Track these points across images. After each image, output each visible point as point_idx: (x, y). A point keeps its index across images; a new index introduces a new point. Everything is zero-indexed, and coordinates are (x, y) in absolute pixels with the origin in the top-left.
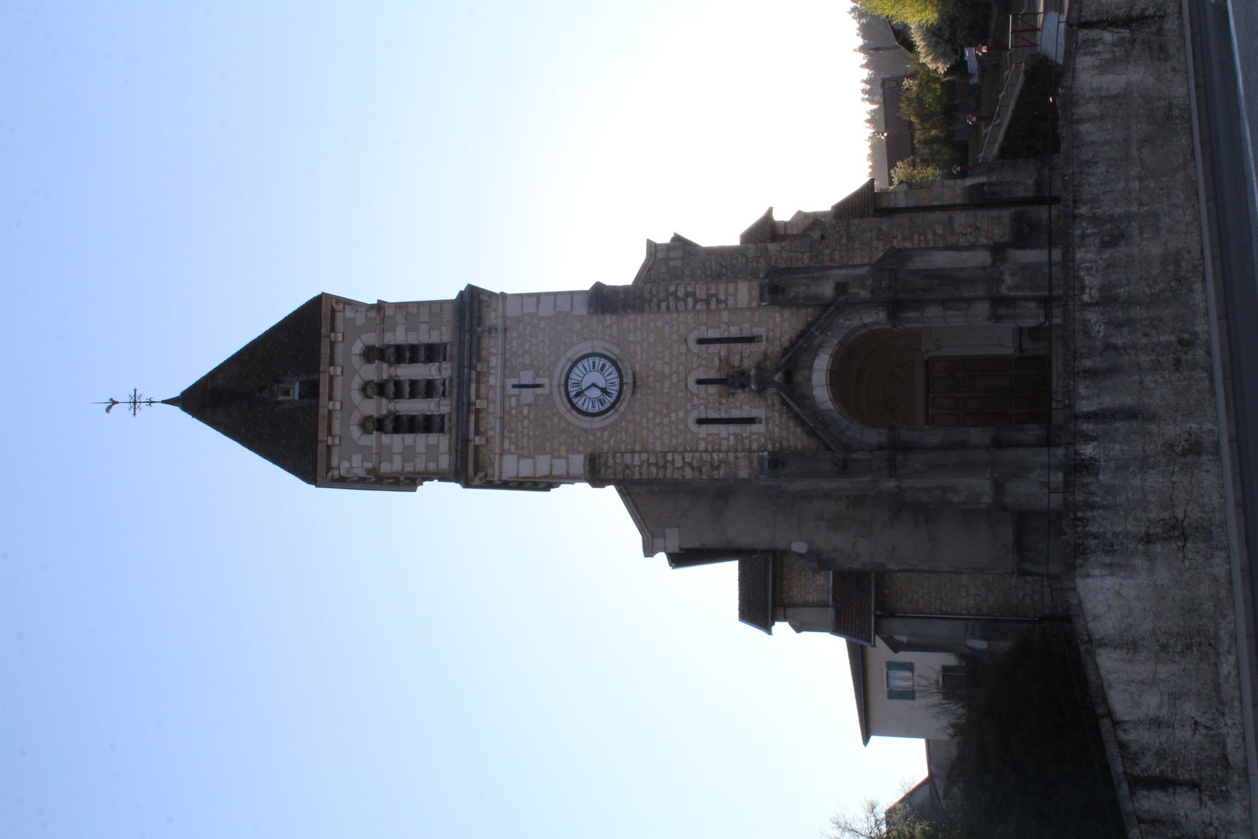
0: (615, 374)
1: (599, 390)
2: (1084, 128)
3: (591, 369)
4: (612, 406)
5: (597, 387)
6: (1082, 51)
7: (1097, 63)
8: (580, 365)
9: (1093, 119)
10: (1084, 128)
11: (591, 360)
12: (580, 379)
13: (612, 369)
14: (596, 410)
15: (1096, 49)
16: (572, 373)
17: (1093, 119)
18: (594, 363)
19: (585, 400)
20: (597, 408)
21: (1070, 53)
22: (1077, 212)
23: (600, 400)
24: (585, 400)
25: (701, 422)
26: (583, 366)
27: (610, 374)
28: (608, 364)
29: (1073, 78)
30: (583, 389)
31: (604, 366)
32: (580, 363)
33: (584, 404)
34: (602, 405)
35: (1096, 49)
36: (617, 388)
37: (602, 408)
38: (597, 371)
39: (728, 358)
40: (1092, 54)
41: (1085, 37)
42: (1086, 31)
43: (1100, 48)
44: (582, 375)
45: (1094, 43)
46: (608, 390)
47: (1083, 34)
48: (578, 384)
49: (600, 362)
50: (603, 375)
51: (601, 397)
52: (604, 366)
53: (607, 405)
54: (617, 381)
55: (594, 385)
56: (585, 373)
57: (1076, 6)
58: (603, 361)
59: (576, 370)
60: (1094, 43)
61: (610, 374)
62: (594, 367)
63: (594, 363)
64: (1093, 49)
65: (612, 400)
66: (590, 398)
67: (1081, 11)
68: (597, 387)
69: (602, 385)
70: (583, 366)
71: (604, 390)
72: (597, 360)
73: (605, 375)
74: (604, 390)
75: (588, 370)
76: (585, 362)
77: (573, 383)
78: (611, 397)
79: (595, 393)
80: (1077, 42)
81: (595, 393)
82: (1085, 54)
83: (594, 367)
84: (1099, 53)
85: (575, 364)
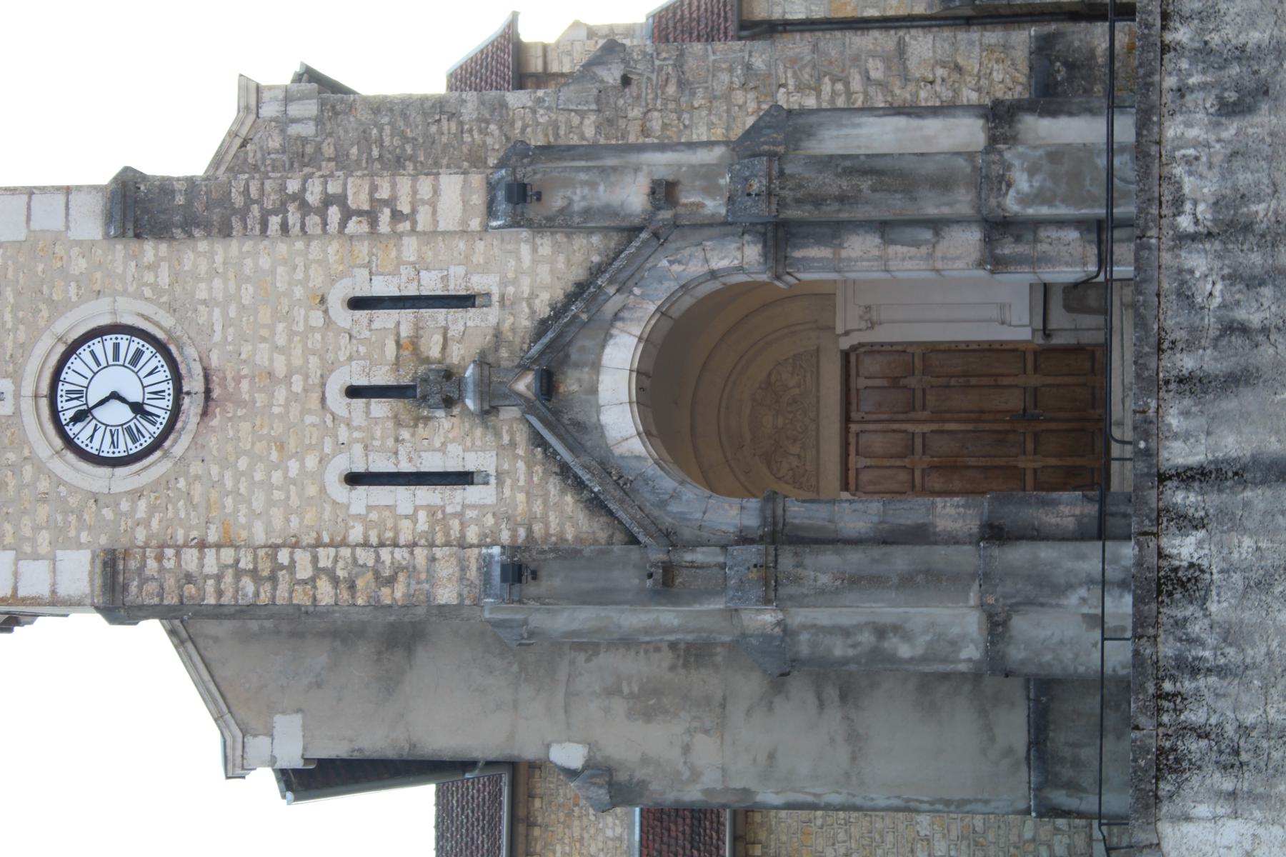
0: (164, 373)
1: (126, 408)
3: (111, 362)
5: (123, 400)
8: (84, 352)
11: (110, 340)
12: (85, 383)
13: (158, 361)
14: (121, 452)
16: (66, 369)
18: (116, 347)
19: (95, 430)
20: (122, 447)
23: (129, 430)
24: (95, 430)
25: (354, 479)
26: (92, 353)
27: (151, 373)
28: (149, 350)
30: (91, 404)
31: (139, 354)
32: (85, 346)
33: (92, 437)
34: (134, 440)
36: (167, 403)
37: (135, 448)
38: (124, 366)
39: (414, 342)
44: (90, 375)
46: (148, 408)
48: (79, 394)
49: (129, 345)
50: (137, 373)
51: (132, 424)
52: (139, 354)
53: (146, 441)
54: (168, 387)
55: (115, 396)
56: (96, 369)
58: (137, 343)
59: (74, 363)
61: (151, 373)
62: (116, 357)
63: (116, 347)
65: (156, 430)
66: (107, 425)
68: (123, 400)
69: (135, 395)
70: (92, 353)
71: (137, 408)
72: (123, 340)
73: (142, 374)
74: (137, 408)
75: (104, 364)
76: (96, 345)
77: (68, 392)
78: (154, 424)
79: (117, 414)
83: (116, 357)
85: (72, 349)
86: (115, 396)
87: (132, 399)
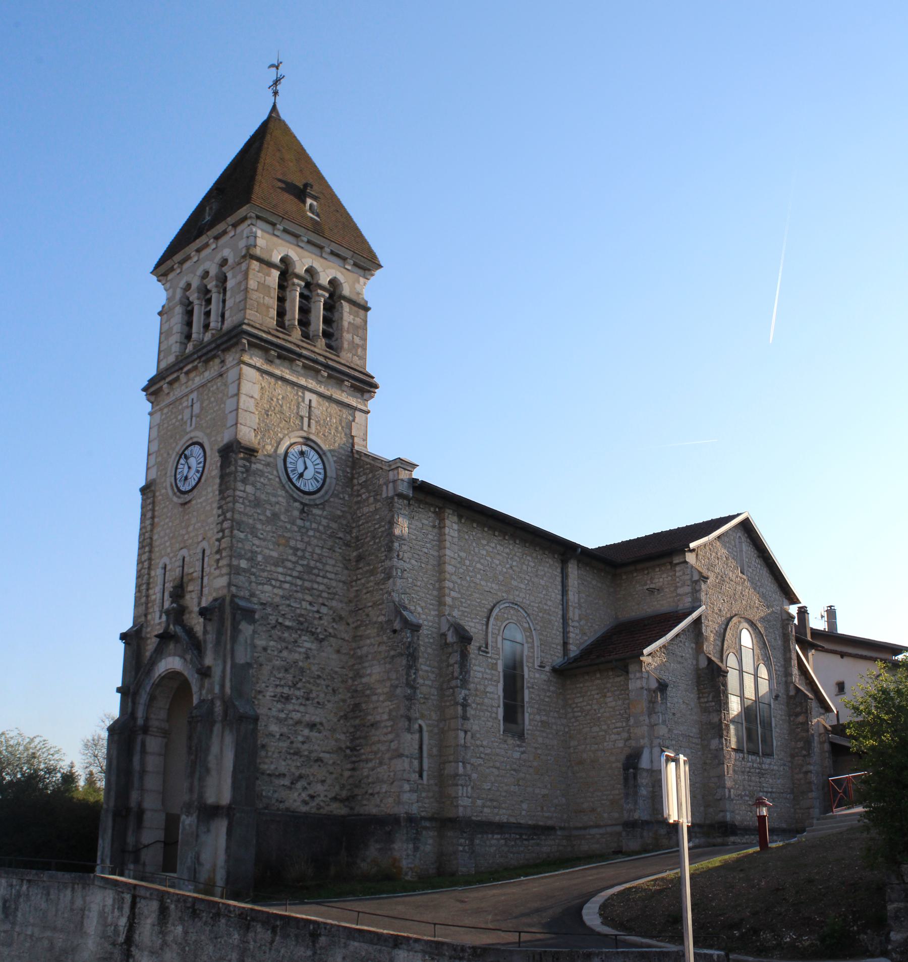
2: (68, 892)
4: (290, 480)
5: (304, 470)
6: (116, 897)
7: (106, 910)
8: (319, 461)
9: (72, 902)
10: (68, 892)
11: (322, 471)
14: (288, 465)
15: (116, 910)
17: (72, 902)
21: (115, 886)
22: (25, 882)
28: (319, 485)
29: (100, 887)
31: (318, 481)
34: (292, 471)
35: (116, 910)
36: (302, 488)
37: (289, 470)
40: (113, 906)
41: (125, 900)
42: (129, 901)
43: (116, 913)
44: (313, 460)
45: (121, 909)
47: (128, 897)
53: (292, 476)
55: (306, 468)
56: (315, 463)
57: (148, 895)
58: (321, 482)
59: (316, 456)
60: (121, 909)
64: (116, 907)
65: (294, 480)
67: (145, 898)
68: (304, 470)
70: (318, 464)
71: (301, 475)
72: (321, 476)
75: (316, 467)
76: (321, 466)
79: (300, 469)
80: (123, 893)
81: (300, 469)
82: (114, 900)
84: (113, 912)
86: (306, 468)
87: (305, 474)
